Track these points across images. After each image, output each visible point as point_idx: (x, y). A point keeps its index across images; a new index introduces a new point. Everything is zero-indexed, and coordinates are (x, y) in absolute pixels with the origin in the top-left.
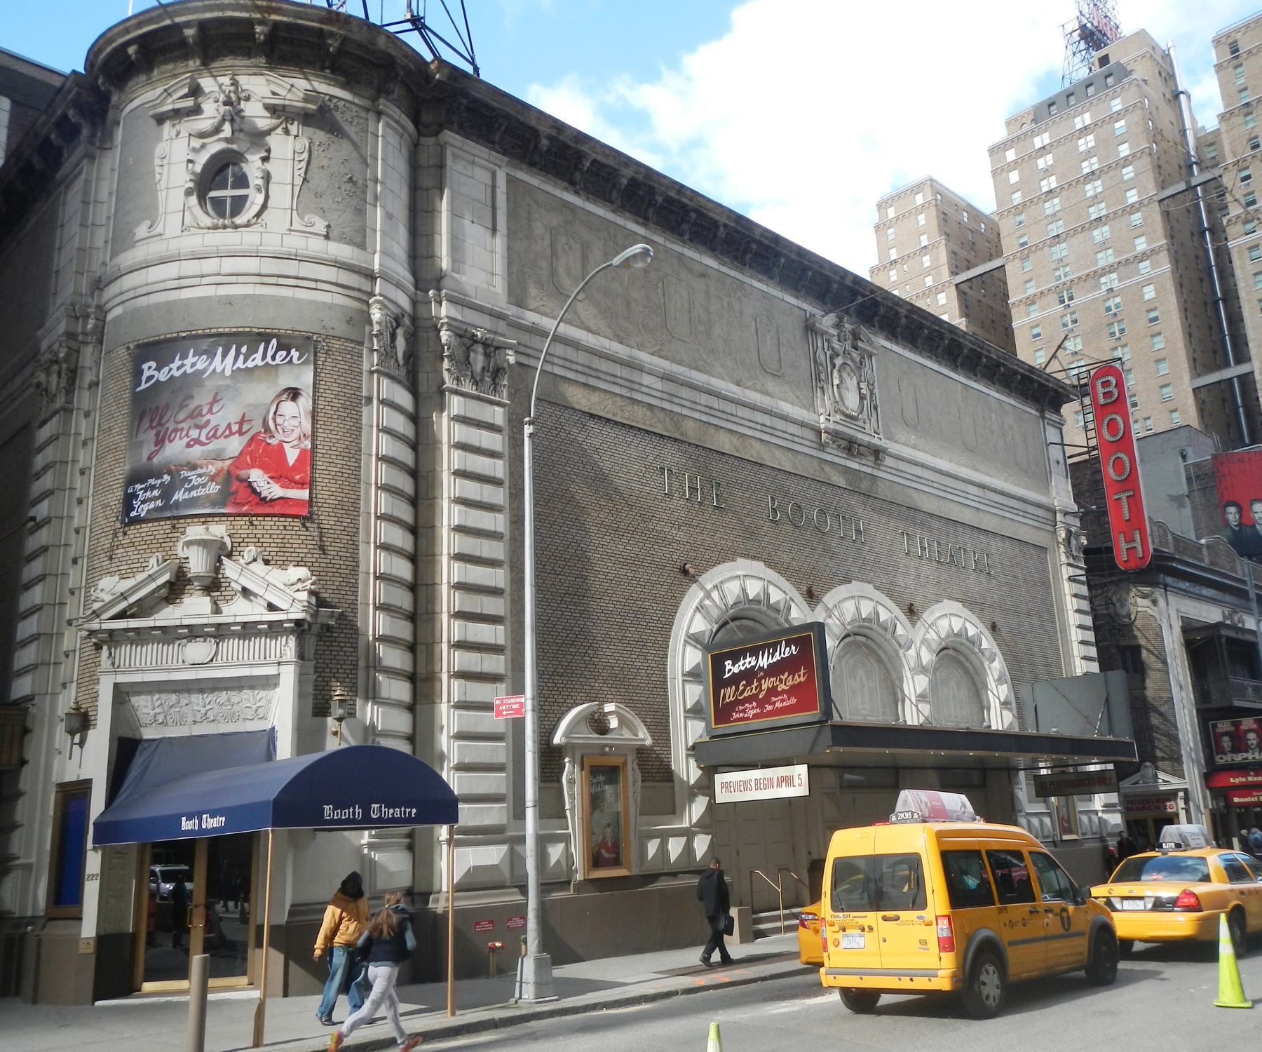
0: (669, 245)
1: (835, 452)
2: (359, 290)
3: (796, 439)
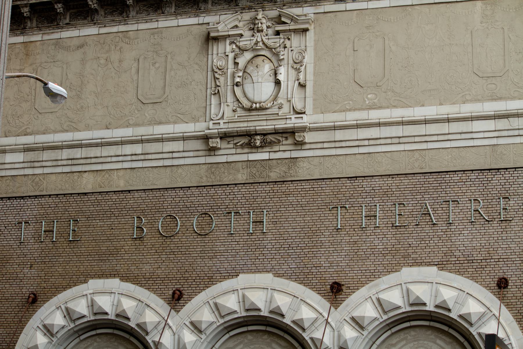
0: (46, 37)
1: (233, 151)
3: (175, 155)
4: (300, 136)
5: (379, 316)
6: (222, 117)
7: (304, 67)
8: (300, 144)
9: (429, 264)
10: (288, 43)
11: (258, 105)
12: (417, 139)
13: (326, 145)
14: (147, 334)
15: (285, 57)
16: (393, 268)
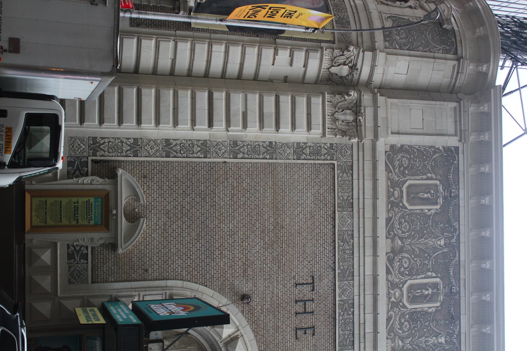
2: (362, 42)
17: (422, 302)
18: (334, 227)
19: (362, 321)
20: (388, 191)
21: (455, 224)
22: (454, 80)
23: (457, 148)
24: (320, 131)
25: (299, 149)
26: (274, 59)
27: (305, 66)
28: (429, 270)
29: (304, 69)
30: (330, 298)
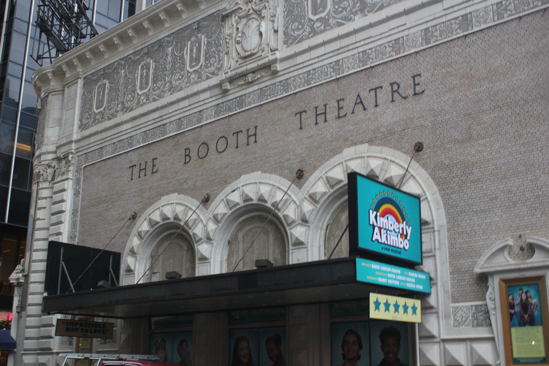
1: (238, 89)
4: (274, 67)
5: (327, 191)
6: (230, 68)
7: (277, 18)
8: (275, 73)
9: (362, 143)
10: (267, 4)
11: (249, 53)
12: (350, 47)
13: (292, 69)
14: (190, 228)
15: (265, 15)
16: (336, 151)
17: (149, 75)
18: (109, 158)
19: (153, 122)
20: (97, 123)
21: (116, 64)
22: (60, 92)
23: (85, 78)
24: (66, 182)
25: (76, 194)
26: (42, 219)
27: (46, 198)
28: (134, 77)
29: (48, 199)
30: (141, 151)
